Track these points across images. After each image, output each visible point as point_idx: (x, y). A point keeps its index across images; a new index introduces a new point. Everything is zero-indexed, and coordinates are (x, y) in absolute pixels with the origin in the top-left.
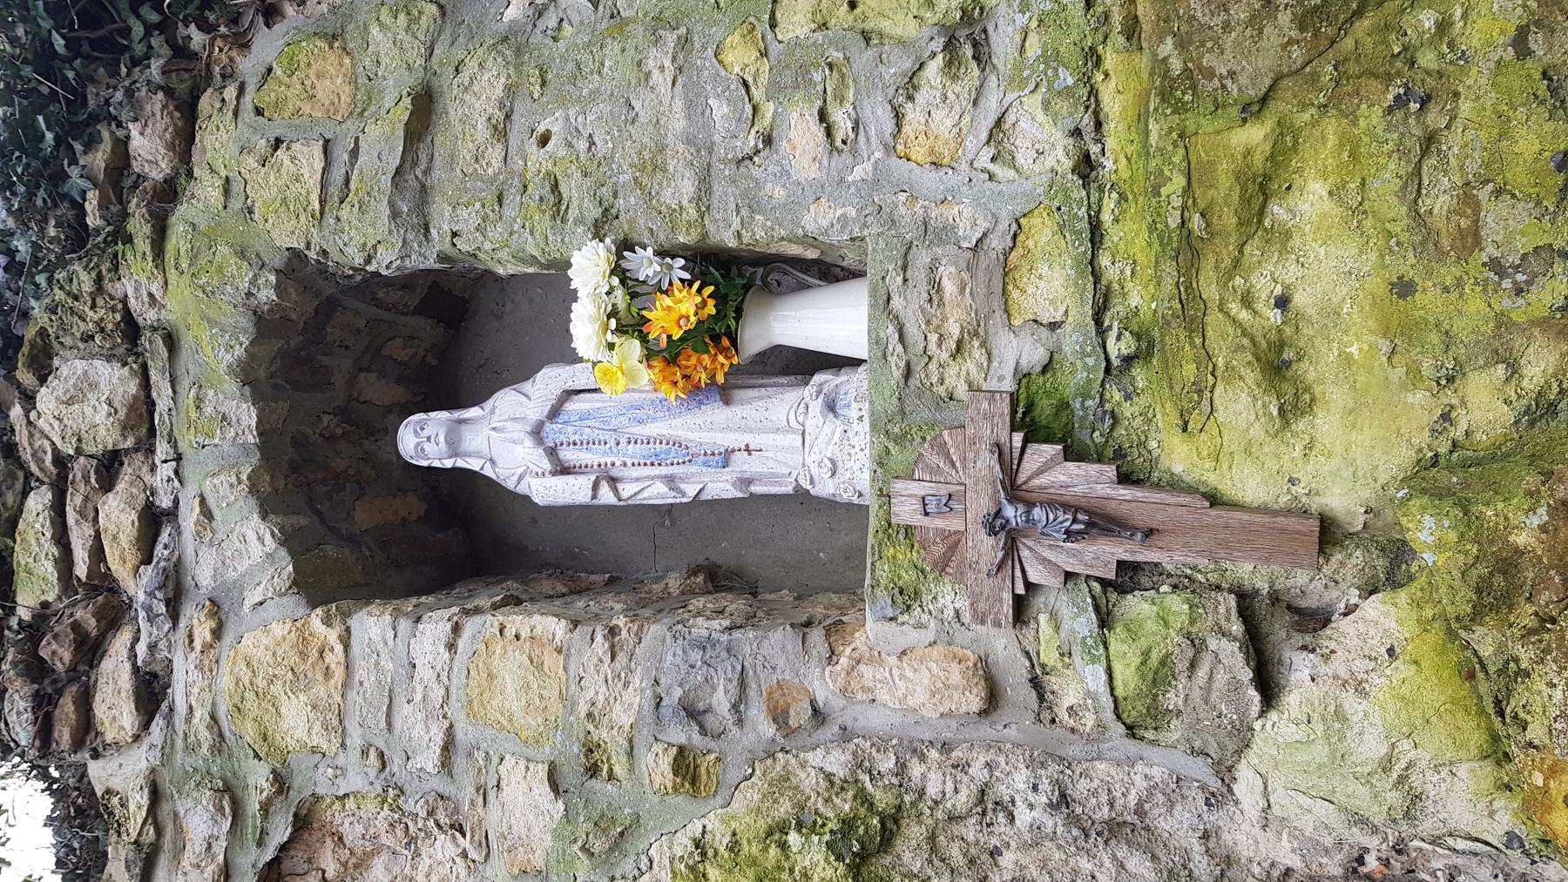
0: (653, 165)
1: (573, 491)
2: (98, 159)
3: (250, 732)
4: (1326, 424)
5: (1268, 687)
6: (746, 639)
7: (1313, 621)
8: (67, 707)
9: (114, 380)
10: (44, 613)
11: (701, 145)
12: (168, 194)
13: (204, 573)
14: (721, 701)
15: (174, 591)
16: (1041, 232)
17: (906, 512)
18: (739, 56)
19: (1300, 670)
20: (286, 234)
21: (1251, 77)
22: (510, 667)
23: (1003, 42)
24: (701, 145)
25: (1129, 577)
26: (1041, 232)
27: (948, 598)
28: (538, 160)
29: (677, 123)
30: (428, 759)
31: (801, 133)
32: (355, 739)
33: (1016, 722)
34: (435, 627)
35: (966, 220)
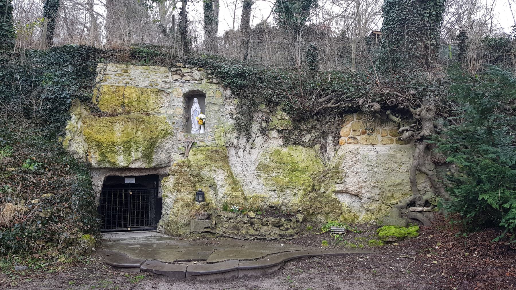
0: (209, 121)
1: (192, 113)
2: (214, 77)
3: (174, 90)
4: (192, 157)
5: (180, 154)
6: (182, 126)
7: (184, 156)
8: (175, 73)
9: (198, 78)
10: (181, 71)
11: (210, 124)
12: (211, 83)
13: (185, 85)
14: (178, 125)
15: (184, 83)
16: (204, 143)
17: (189, 136)
18: (216, 126)
19: (181, 156)
20: (207, 93)
21: (207, 153)
22: (179, 110)
23: (213, 142)
24: (210, 124)
25: (185, 148)
26: (204, 143)
27: (184, 138)
28: (211, 113)
29: (212, 122)
30: (173, 104)
31: (210, 130)
32: (174, 98)
33: (178, 142)
34: (181, 104)
35: (205, 139)
